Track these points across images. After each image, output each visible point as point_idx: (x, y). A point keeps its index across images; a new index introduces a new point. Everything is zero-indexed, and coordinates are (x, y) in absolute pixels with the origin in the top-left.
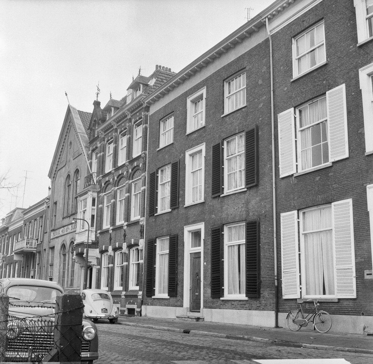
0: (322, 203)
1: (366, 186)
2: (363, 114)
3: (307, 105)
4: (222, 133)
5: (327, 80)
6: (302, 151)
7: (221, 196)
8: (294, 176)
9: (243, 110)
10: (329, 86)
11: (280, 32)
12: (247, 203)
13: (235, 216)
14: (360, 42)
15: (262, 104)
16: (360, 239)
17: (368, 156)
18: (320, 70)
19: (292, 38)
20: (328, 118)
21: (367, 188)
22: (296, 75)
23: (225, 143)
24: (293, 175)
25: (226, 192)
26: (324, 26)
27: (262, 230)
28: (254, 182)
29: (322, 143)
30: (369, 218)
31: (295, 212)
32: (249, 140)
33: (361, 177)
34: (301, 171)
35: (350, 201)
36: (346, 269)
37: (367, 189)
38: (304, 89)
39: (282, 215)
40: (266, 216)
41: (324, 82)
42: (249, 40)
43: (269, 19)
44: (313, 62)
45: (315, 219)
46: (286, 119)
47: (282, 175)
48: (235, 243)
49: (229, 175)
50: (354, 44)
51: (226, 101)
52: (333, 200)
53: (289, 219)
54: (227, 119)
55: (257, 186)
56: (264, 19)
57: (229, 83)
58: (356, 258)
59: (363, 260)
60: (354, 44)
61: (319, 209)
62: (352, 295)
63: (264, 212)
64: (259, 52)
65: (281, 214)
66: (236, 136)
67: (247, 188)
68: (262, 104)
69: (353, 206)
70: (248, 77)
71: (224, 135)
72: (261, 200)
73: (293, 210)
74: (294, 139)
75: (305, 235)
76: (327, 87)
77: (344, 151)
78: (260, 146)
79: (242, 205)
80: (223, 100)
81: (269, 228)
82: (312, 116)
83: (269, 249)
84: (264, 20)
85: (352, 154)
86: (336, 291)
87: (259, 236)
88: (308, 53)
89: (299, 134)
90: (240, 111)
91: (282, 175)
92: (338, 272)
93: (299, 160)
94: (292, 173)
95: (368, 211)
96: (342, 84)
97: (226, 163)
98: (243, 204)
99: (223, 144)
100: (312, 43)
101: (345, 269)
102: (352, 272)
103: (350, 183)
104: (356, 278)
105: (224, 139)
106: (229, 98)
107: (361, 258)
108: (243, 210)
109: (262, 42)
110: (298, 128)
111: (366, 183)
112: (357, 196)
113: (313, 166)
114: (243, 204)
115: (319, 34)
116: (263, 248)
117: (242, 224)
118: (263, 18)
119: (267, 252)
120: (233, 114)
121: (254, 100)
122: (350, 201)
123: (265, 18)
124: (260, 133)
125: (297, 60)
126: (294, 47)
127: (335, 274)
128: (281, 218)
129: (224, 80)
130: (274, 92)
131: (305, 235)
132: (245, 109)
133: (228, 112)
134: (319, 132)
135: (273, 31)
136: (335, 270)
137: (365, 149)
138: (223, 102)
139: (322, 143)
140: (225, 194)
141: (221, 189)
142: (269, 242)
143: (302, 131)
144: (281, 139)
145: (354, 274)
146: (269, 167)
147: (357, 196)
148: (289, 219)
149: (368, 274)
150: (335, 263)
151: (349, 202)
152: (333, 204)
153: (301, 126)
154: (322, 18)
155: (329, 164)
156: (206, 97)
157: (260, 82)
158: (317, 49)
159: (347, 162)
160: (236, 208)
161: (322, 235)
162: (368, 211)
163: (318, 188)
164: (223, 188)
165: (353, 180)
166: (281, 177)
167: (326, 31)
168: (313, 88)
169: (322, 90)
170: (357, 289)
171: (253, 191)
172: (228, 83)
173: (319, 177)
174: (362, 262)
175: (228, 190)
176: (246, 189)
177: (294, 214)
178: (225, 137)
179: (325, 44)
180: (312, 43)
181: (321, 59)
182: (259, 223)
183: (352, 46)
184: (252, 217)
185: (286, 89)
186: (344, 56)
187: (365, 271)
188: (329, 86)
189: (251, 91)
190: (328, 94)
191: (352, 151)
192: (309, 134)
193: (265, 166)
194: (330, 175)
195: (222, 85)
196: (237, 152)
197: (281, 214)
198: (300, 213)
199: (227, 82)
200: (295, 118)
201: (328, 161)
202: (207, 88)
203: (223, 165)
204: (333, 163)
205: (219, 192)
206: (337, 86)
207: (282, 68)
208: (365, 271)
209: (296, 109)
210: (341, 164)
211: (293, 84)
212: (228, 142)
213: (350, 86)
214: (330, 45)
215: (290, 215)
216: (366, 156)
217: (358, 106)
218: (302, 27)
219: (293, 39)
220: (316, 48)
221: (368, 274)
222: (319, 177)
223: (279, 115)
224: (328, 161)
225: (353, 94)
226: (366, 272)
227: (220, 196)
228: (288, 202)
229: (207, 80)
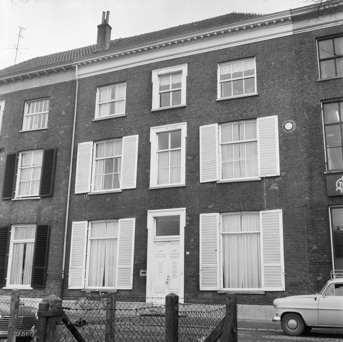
0: (110, 218)
1: (147, 211)
2: (150, 160)
3: (105, 142)
4: (18, 146)
5: (124, 128)
6: (95, 176)
7: (12, 200)
8: (88, 194)
9: (44, 131)
10: (125, 133)
11: (87, 78)
12: (40, 209)
13: (26, 219)
14: (154, 109)
15: (63, 131)
16: (139, 247)
17: (151, 190)
18: (119, 119)
19: (97, 87)
20: (122, 156)
21: (148, 213)
22: (97, 117)
23: (20, 155)
24: (87, 193)
25: (17, 196)
26: (126, 87)
27: (52, 233)
28: (49, 194)
29: (113, 173)
30: (147, 233)
31: (86, 222)
32: (47, 158)
33: (144, 204)
34: (93, 192)
35: (134, 220)
36: (126, 268)
37: (148, 213)
38: (103, 129)
39: (74, 223)
40: (57, 222)
41: (122, 129)
42: (56, 75)
43: (78, 66)
44: (112, 111)
45: (102, 229)
46: (86, 149)
47: (76, 192)
48: (31, 241)
49: (20, 183)
50: (148, 109)
51: (25, 119)
52: (119, 217)
53: (80, 229)
54: (26, 135)
55: (51, 196)
56: (75, 64)
57: (29, 105)
58: (134, 261)
59: (140, 262)
60: (148, 109)
61: (106, 222)
62: (129, 287)
63: (57, 219)
64: (65, 88)
65: (73, 222)
66: (33, 152)
67: (41, 197)
68: (63, 131)
69: (136, 223)
70: (51, 106)
71: (20, 148)
72: (53, 209)
73: (84, 221)
74: (91, 166)
75: (91, 240)
76: (124, 133)
77: (133, 183)
78: (57, 164)
79: (34, 210)
80: (23, 117)
81: (60, 232)
82: (109, 150)
83: (58, 249)
84: (74, 65)
85: (139, 186)
86: (116, 284)
87: (49, 238)
88: (109, 103)
89: (94, 162)
90: (40, 132)
91: (76, 192)
92: (119, 270)
93: (93, 182)
94: (86, 192)
95: (147, 228)
96: (136, 134)
97: (19, 171)
98: (35, 209)
99: (18, 156)
100: (113, 97)
101: (125, 268)
102: (131, 271)
103: (135, 207)
104: (133, 275)
105: (19, 151)
106: (28, 117)
107: (138, 261)
108: (34, 214)
109: (69, 81)
110: (94, 158)
111: (147, 209)
112: (139, 217)
113: (104, 189)
114: (35, 209)
115: (121, 92)
116: (52, 248)
117: (33, 226)
118: (73, 63)
119: (56, 251)
120: (32, 132)
121: (55, 126)
122: (134, 220)
123: (76, 64)
124: (58, 154)
125: (99, 105)
126: (98, 94)
127: (117, 271)
128: (73, 226)
129: (25, 101)
130: (76, 125)
131: (91, 240)
132: (46, 131)
133: (25, 129)
134: (111, 164)
135: (81, 76)
136: (117, 269)
137: (149, 184)
138: (22, 120)
139: (113, 173)
140: (15, 199)
141: (13, 194)
142: (58, 244)
143: (97, 160)
144: (79, 163)
145: (132, 272)
146: (65, 183)
147: (139, 217)
148: (80, 229)
149: (142, 273)
150: (117, 263)
151: (133, 221)
152: (120, 220)
153: (96, 157)
154: (125, 81)
155: (119, 190)
156: (3, 110)
157: (63, 113)
158: (117, 102)
159: (135, 191)
160: (27, 212)
161: (106, 242)
162: (147, 228)
163: (105, 207)
164: (15, 193)
165: (137, 205)
166: (76, 193)
167: (127, 91)
168: (108, 131)
169: (119, 134)
170: (133, 283)
171: (45, 201)
172: (28, 104)
173: (110, 199)
174: (138, 264)
175: (19, 195)
176: (39, 198)
177: (85, 224)
178: (21, 150)
179: (125, 101)
180: (113, 97)
181: (121, 110)
182: (51, 227)
183: (147, 110)
184: (44, 221)
185: (87, 125)
186: (140, 115)
187: (141, 270)
188: (125, 133)
189: (53, 116)
190: (125, 139)
191: (139, 184)
192: (102, 165)
193: (61, 182)
194: (119, 198)
195: (23, 104)
196: (32, 164)
197: (73, 222)
198: (89, 223)
199: (27, 103)
200: (93, 149)
201: (119, 187)
202: (6, 103)
203: (17, 173)
204: (123, 190)
205: (11, 196)
206: (132, 135)
207: (85, 107)
208: (141, 270)
209: (94, 143)
210: (129, 192)
211: (94, 123)
212: (22, 154)
213: (142, 138)
214: (129, 103)
215: (82, 224)
216: (150, 190)
217: (147, 153)
218: (106, 82)
219: (97, 88)
220: (116, 101)
221: (142, 273)
222: (110, 199)
223: (79, 144)
224: (119, 187)
225: (144, 144)
226: (141, 271)
227: (11, 199)
228: (80, 213)
229: (10, 94)
